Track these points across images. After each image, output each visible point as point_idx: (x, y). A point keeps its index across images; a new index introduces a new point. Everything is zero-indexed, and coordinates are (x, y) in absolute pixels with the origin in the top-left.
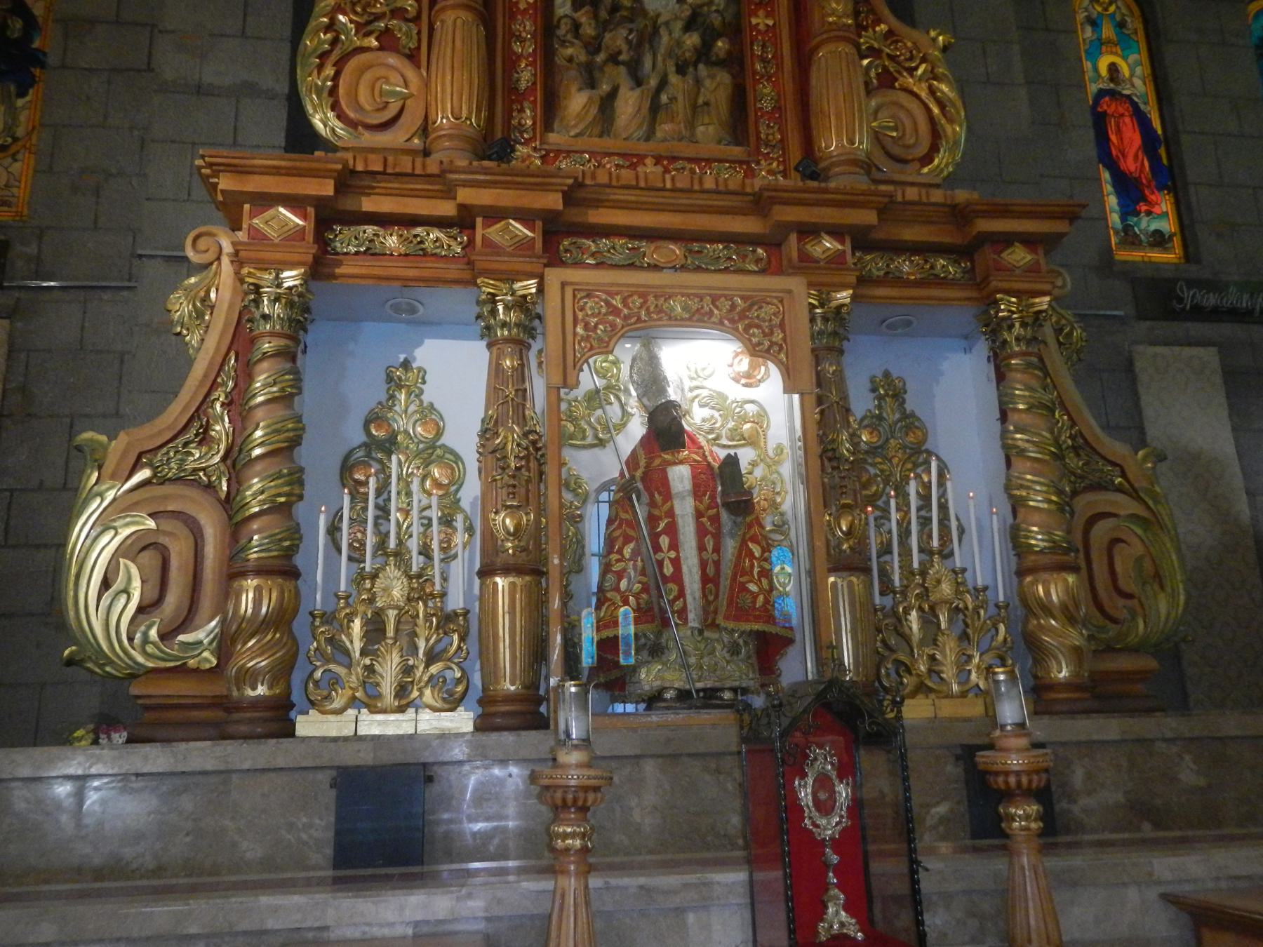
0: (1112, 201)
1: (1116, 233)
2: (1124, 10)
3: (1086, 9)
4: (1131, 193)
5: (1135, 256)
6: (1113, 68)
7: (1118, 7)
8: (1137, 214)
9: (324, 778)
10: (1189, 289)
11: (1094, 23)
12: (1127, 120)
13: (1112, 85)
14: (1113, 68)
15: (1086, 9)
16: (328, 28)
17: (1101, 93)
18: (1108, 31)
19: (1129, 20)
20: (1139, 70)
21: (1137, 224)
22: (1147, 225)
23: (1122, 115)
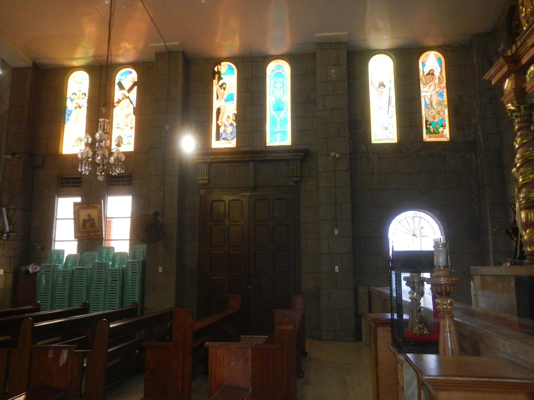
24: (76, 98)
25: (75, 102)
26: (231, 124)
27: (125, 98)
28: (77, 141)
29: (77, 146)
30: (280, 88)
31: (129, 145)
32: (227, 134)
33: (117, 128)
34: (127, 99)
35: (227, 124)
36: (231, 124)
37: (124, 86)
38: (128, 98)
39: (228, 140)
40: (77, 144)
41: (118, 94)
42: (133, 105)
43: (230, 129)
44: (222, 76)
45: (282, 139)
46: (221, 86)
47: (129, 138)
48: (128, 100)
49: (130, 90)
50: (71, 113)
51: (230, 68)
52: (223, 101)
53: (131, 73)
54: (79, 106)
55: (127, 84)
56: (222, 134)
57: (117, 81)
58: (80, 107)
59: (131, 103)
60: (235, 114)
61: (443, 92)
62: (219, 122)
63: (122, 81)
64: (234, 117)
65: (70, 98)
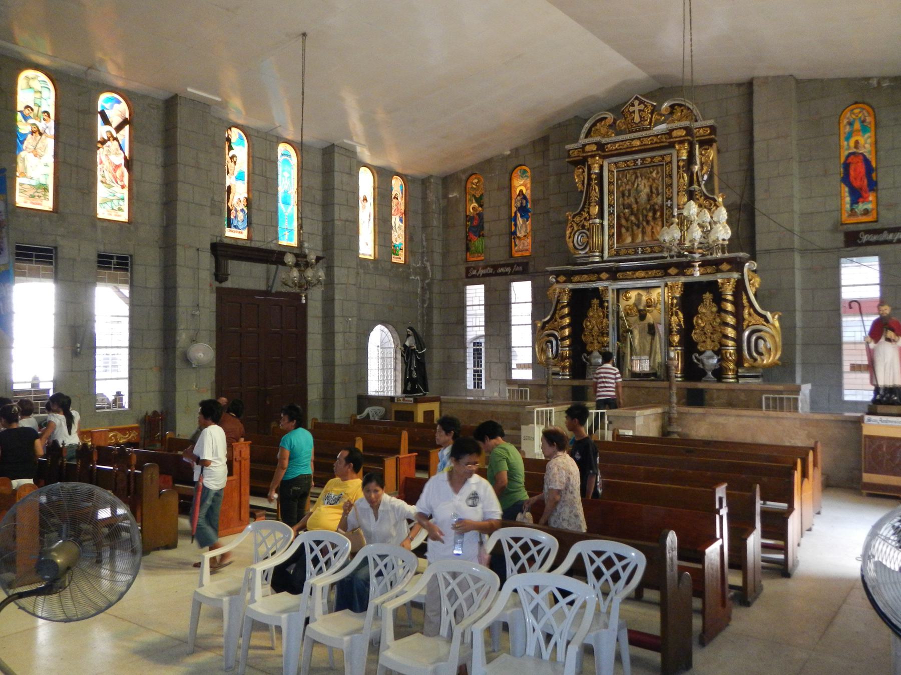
0: (848, 199)
1: (848, 212)
2: (866, 114)
3: (848, 118)
4: (857, 196)
5: (854, 220)
6: (857, 142)
7: (863, 114)
8: (857, 203)
9: (569, 387)
10: (865, 234)
11: (850, 124)
12: (860, 164)
13: (855, 150)
14: (857, 142)
15: (848, 118)
16: (571, 226)
17: (850, 154)
18: (857, 125)
19: (867, 118)
20: (869, 141)
21: (857, 207)
22: (861, 207)
23: (858, 162)
24: (32, 115)
25: (31, 121)
26: (242, 210)
27: (111, 139)
28: (39, 188)
29: (38, 196)
30: (288, 178)
31: (120, 213)
32: (238, 221)
33: (102, 182)
34: (115, 141)
35: (239, 209)
36: (242, 210)
37: (110, 120)
38: (116, 139)
39: (239, 229)
40: (40, 194)
41: (102, 131)
42: (124, 153)
43: (241, 216)
44: (232, 145)
45: (290, 239)
46: (232, 158)
47: (121, 202)
48: (115, 142)
49: (119, 128)
50: (25, 139)
51: (240, 138)
52: (233, 177)
53: (119, 102)
54: (39, 130)
55: (115, 120)
56: (233, 219)
57: (99, 109)
58: (41, 134)
59: (121, 149)
60: (246, 198)
61: (402, 217)
62: (229, 204)
63: (106, 111)
64: (245, 201)
65: (21, 112)
